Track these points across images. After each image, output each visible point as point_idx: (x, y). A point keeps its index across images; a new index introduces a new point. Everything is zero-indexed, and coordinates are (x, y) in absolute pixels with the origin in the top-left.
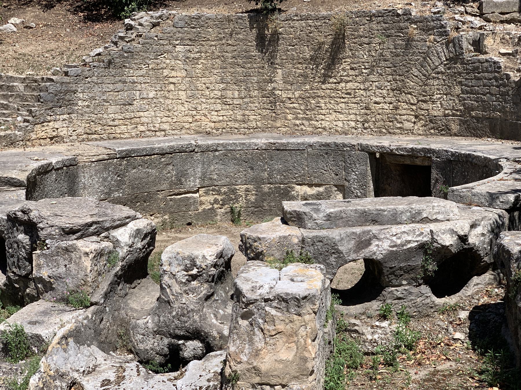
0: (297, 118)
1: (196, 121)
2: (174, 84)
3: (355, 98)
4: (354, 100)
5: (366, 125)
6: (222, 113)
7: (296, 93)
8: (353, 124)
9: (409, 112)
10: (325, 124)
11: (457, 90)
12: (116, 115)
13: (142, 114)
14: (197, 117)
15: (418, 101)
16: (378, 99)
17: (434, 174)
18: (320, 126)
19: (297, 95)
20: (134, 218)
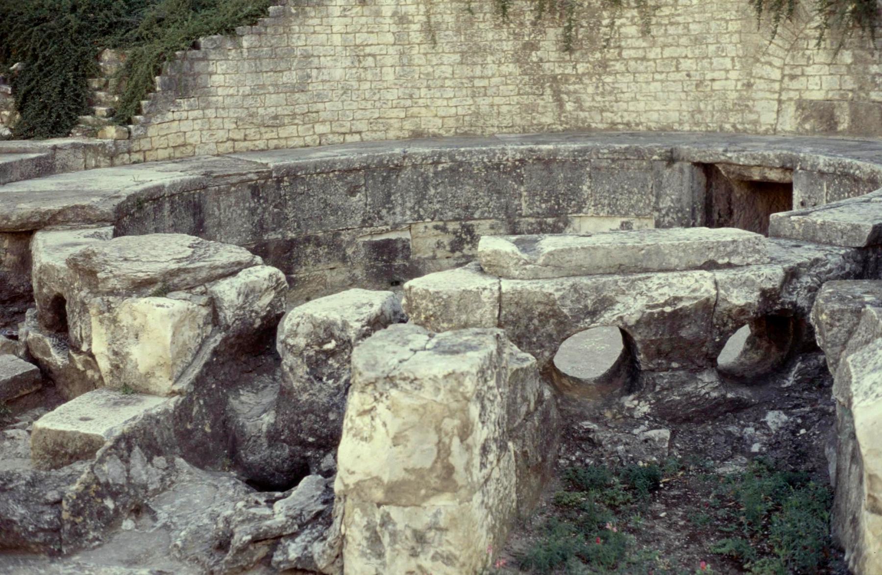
2: (374, 56)
3: (678, 70)
4: (678, 76)
5: (698, 116)
7: (578, 66)
9: (768, 95)
12: (279, 109)
13: (320, 106)
14: (415, 110)
15: (783, 76)
16: (716, 75)
18: (619, 120)
20: (250, 264)
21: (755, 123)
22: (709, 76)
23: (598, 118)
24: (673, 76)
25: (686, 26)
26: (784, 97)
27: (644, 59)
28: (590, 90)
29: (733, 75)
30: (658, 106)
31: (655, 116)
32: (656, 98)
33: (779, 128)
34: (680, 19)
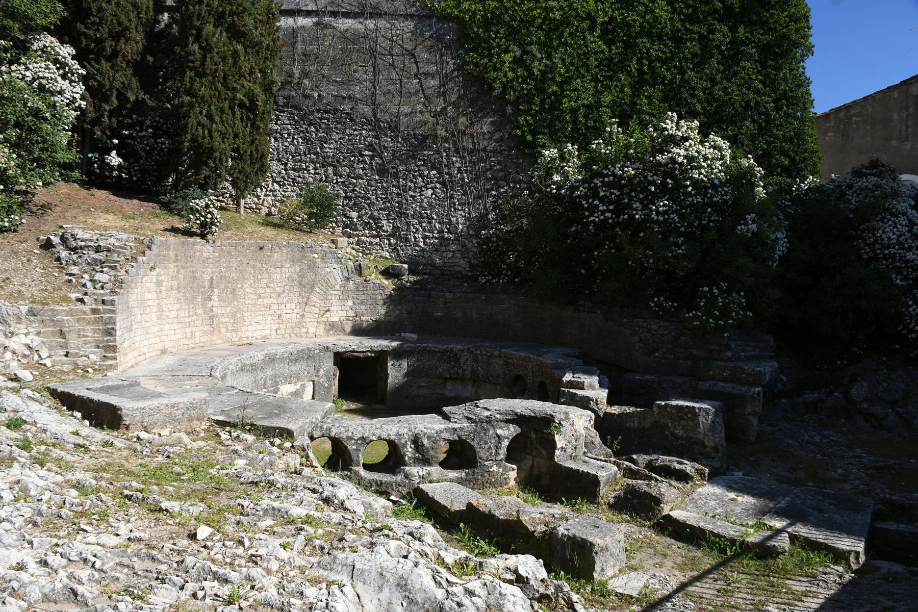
1: (162, 341)
2: (149, 306)
6: (177, 332)
8: (268, 332)
10: (249, 334)
11: (350, 303)
16: (288, 311)
19: (228, 309)
22: (285, 311)
23: (234, 335)
24: (268, 312)
25: (274, 288)
30: (260, 327)
31: (259, 333)
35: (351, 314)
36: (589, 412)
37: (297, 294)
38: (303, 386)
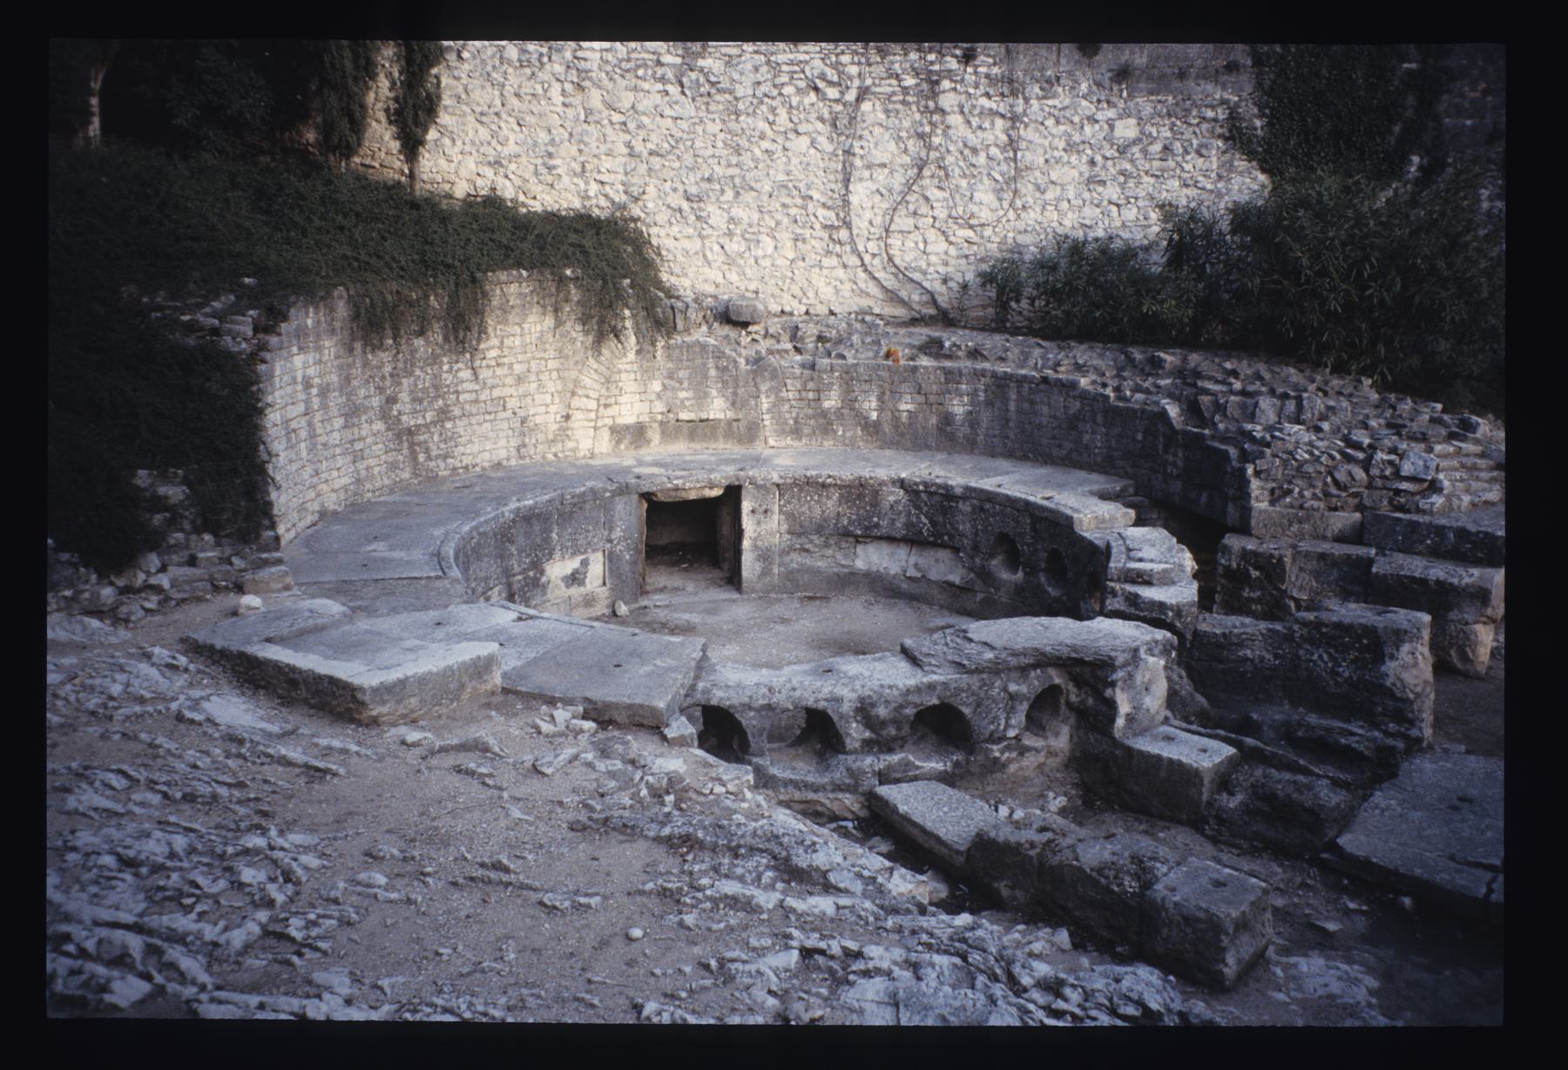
0: (429, 458)
10: (467, 460)
11: (656, 386)
17: (746, 506)
21: (574, 450)
23: (442, 465)
24: (502, 415)
26: (600, 424)
27: (476, 401)
28: (436, 438)
29: (553, 409)
31: (487, 456)
32: (487, 438)
33: (596, 451)
34: (506, 360)
35: (659, 407)
36: (1169, 635)
37: (555, 375)
38: (585, 563)
